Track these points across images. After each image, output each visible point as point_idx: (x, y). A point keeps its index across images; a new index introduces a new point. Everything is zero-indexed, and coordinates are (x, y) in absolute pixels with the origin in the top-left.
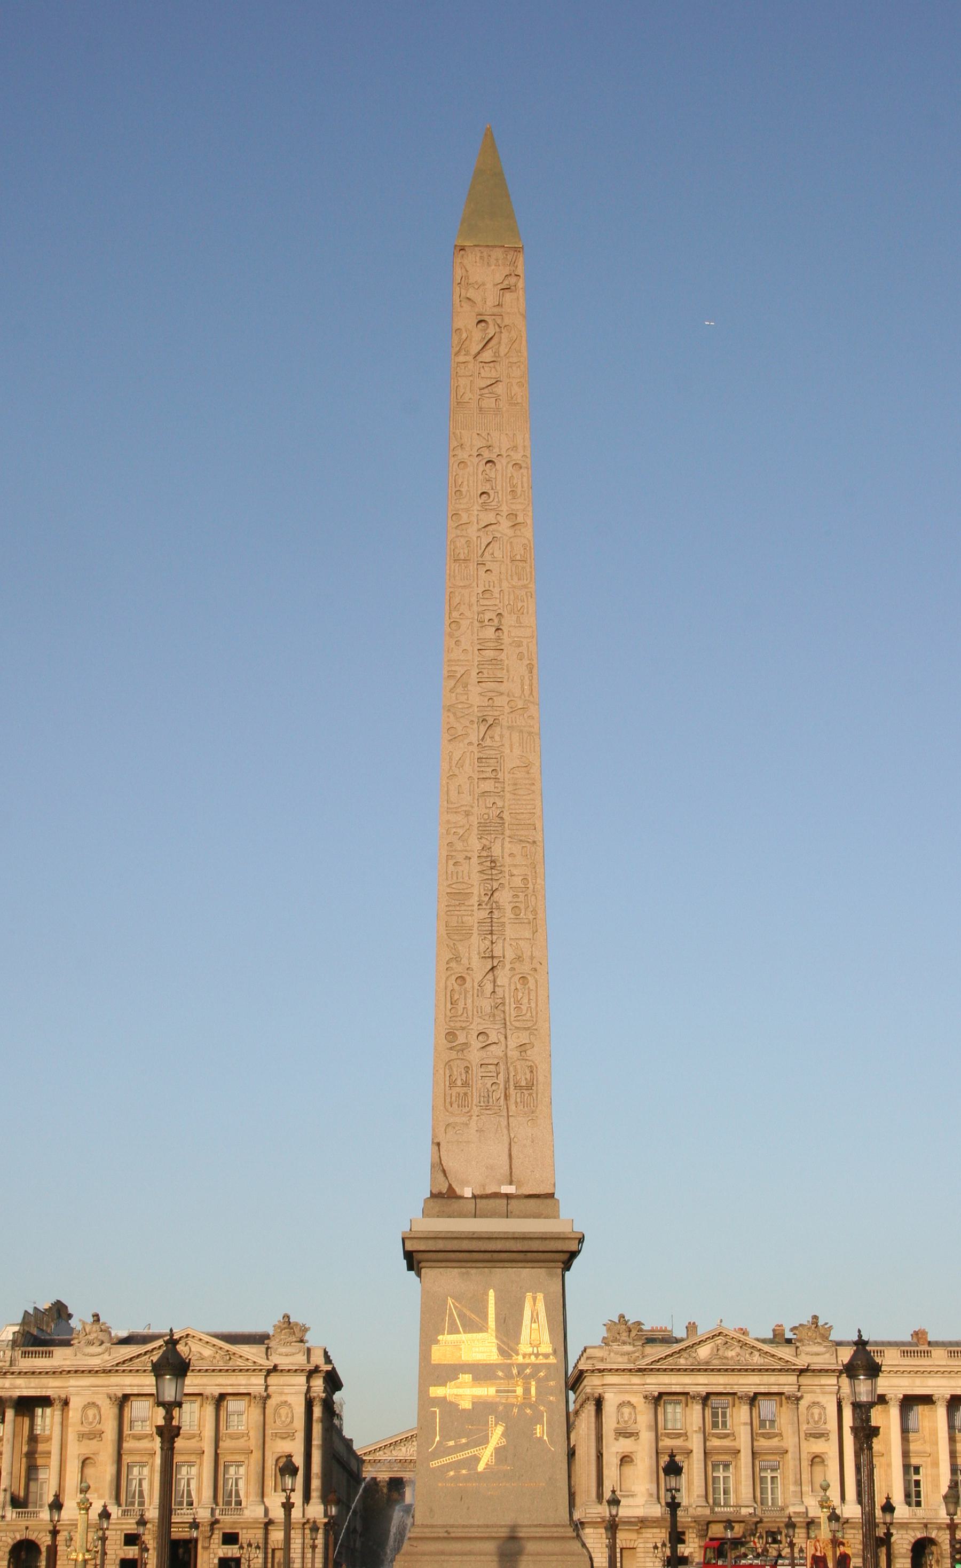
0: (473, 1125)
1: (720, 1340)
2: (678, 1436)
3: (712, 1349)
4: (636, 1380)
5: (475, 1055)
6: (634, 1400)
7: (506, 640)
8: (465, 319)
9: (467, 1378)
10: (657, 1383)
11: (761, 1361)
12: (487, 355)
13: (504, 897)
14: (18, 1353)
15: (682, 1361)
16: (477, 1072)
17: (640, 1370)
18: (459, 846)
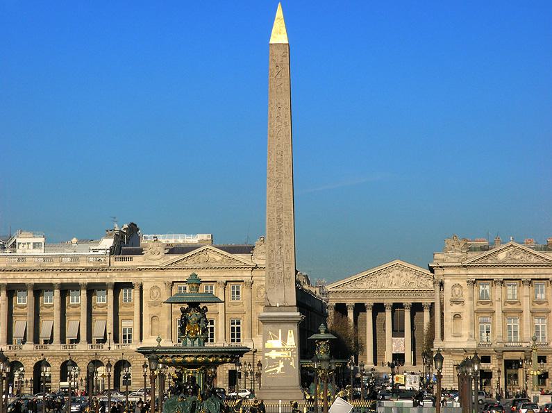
0: (276, 289)
1: (511, 250)
2: (488, 303)
3: (507, 254)
4: (463, 272)
5: (276, 270)
6: (461, 283)
7: (284, 158)
8: (272, 66)
9: (274, 351)
10: (474, 274)
11: (536, 261)
12: (278, 76)
13: (283, 229)
14: (112, 258)
15: (489, 261)
16: (276, 273)
17: (464, 266)
18: (272, 215)
